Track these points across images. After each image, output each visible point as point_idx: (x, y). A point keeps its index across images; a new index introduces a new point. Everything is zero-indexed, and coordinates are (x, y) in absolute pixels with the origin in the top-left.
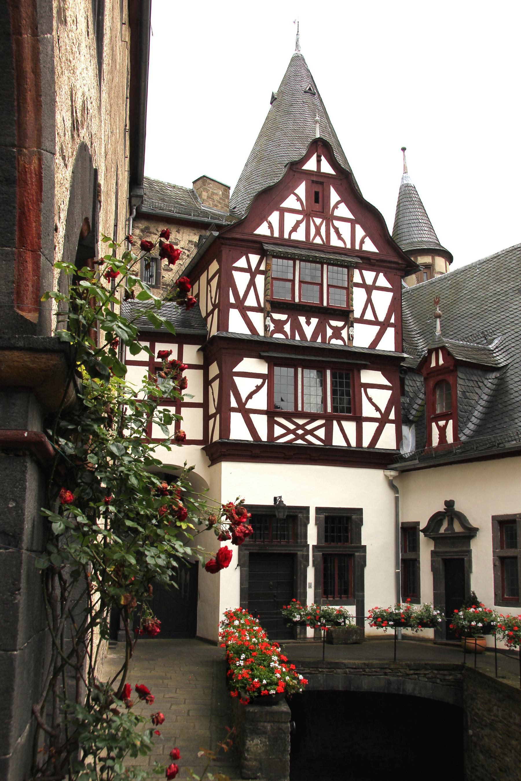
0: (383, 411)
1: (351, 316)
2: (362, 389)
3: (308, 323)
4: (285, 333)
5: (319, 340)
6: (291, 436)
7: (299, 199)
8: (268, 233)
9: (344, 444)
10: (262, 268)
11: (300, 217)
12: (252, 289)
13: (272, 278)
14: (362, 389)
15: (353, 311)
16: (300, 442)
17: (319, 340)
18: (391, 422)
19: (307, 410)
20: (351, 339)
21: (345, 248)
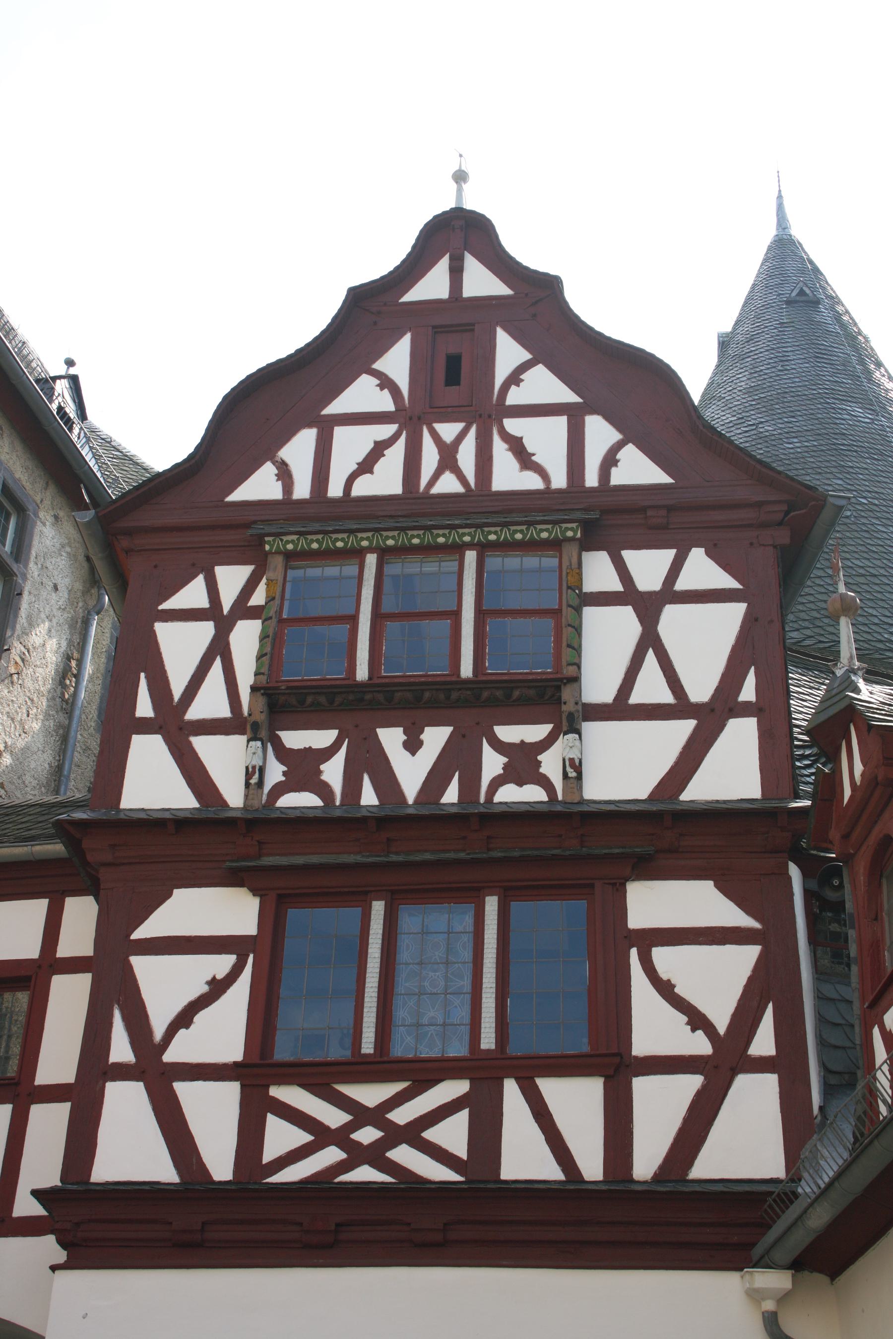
0: (721, 1026)
1: (566, 694)
2: (634, 952)
3: (413, 745)
4: (323, 790)
5: (451, 795)
6: (332, 1155)
7: (386, 383)
8: (274, 491)
9: (552, 1172)
10: (258, 598)
11: (386, 431)
12: (217, 668)
13: (281, 621)
14: (634, 952)
15: (576, 679)
16: (365, 1174)
17: (451, 795)
18: (761, 1065)
19: (400, 1048)
20: (572, 774)
21: (548, 493)
